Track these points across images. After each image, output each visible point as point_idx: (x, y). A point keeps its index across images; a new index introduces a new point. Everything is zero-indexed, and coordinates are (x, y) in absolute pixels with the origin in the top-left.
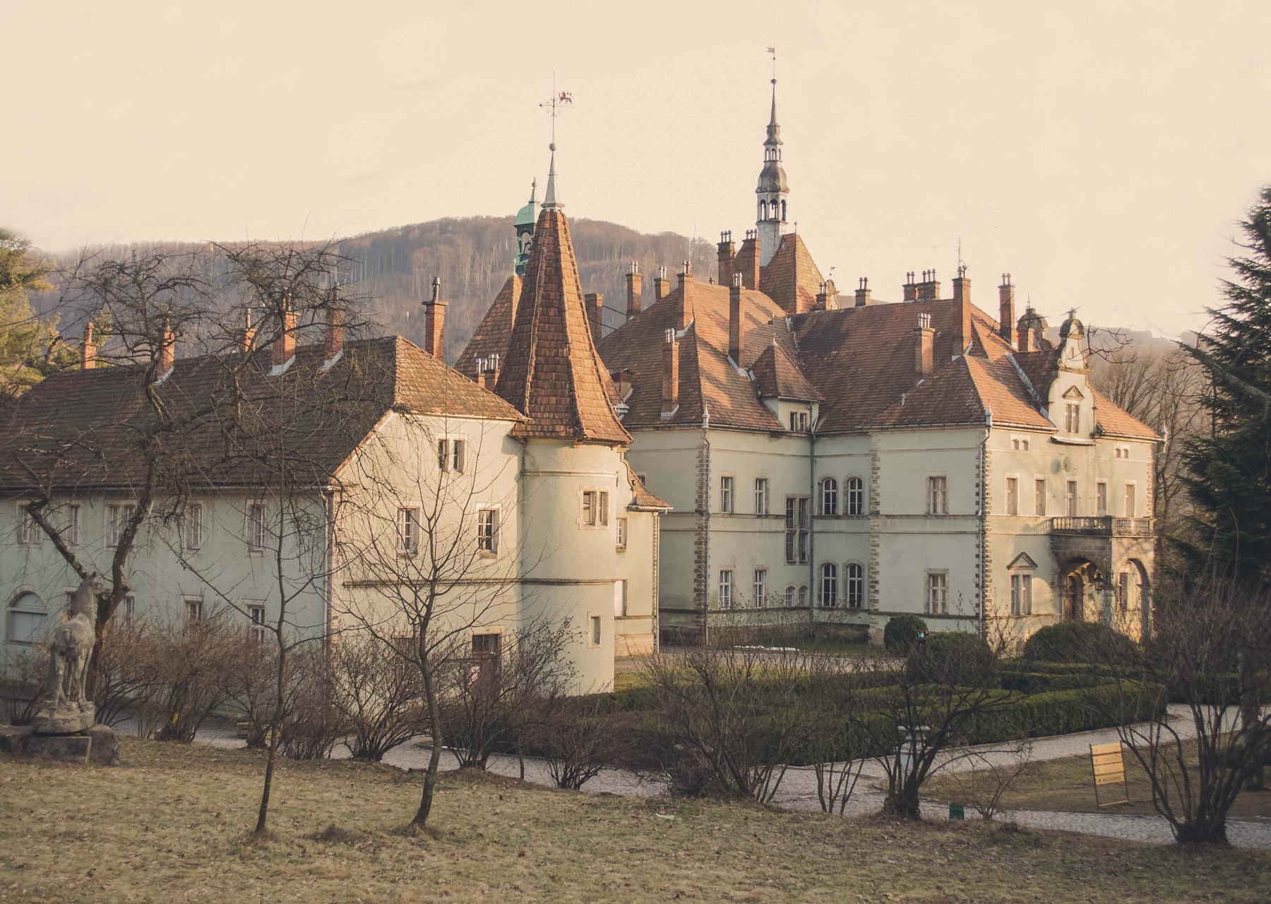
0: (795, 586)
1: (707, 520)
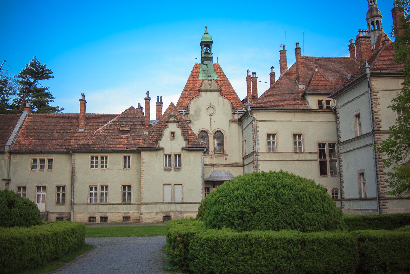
0: (328, 188)
1: (257, 155)
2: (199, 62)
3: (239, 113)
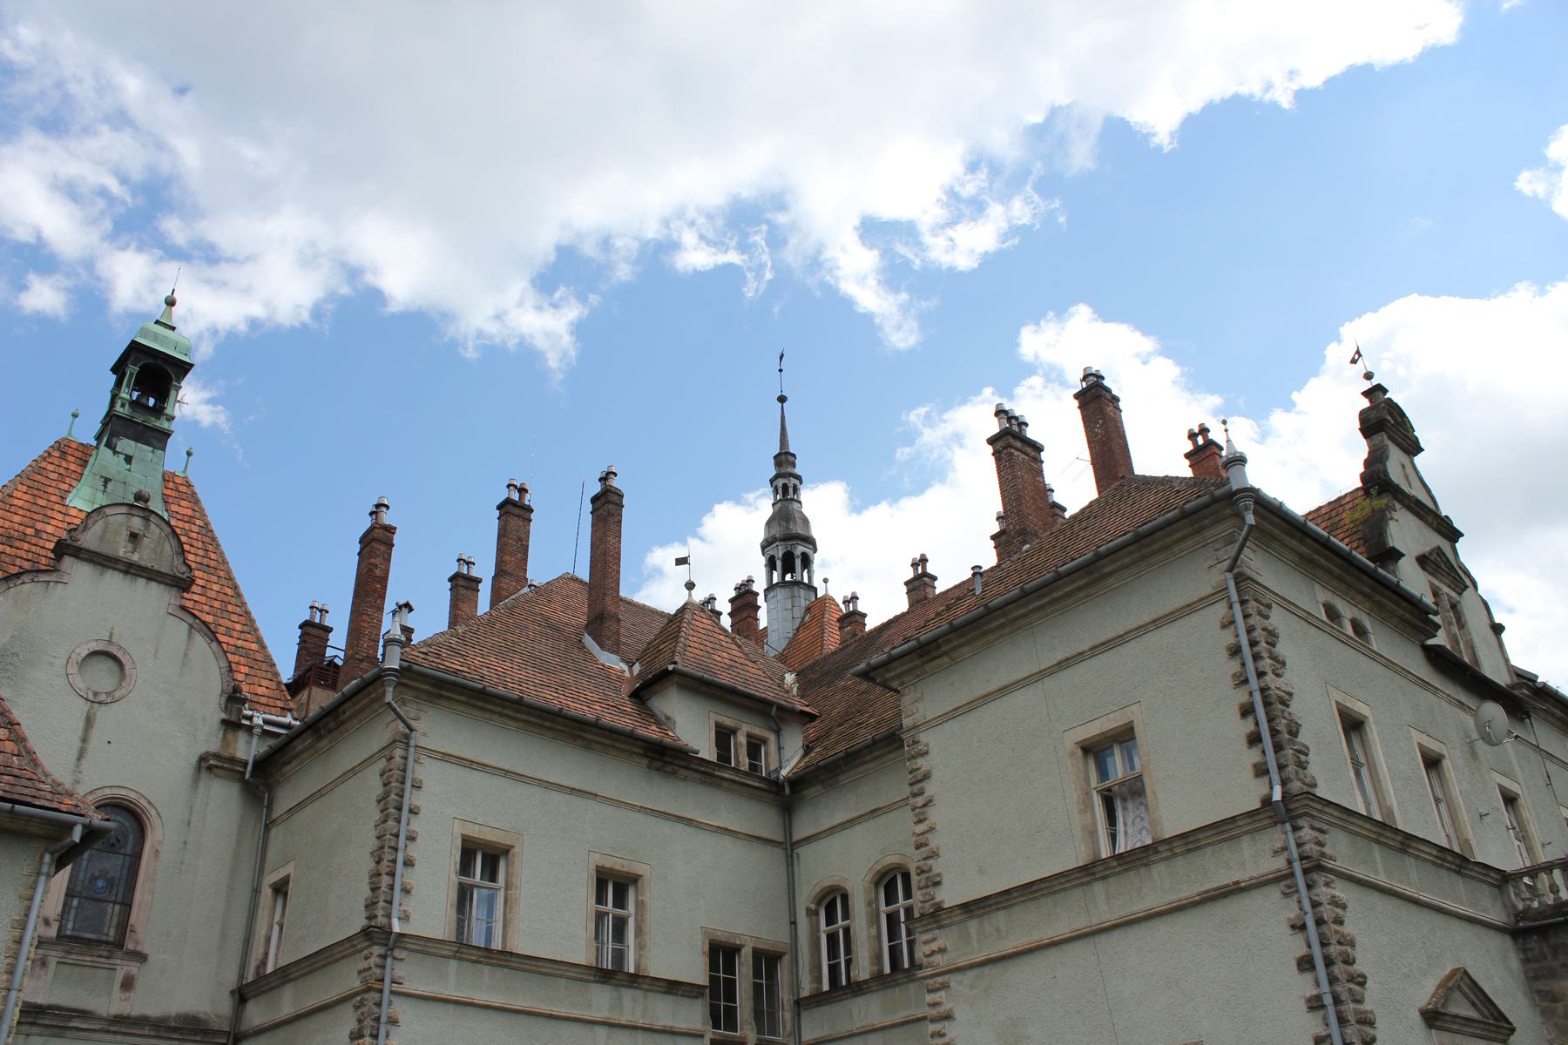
2: (86, 431)
3: (265, 733)
